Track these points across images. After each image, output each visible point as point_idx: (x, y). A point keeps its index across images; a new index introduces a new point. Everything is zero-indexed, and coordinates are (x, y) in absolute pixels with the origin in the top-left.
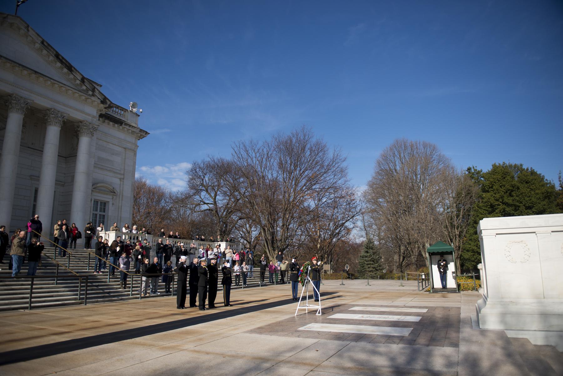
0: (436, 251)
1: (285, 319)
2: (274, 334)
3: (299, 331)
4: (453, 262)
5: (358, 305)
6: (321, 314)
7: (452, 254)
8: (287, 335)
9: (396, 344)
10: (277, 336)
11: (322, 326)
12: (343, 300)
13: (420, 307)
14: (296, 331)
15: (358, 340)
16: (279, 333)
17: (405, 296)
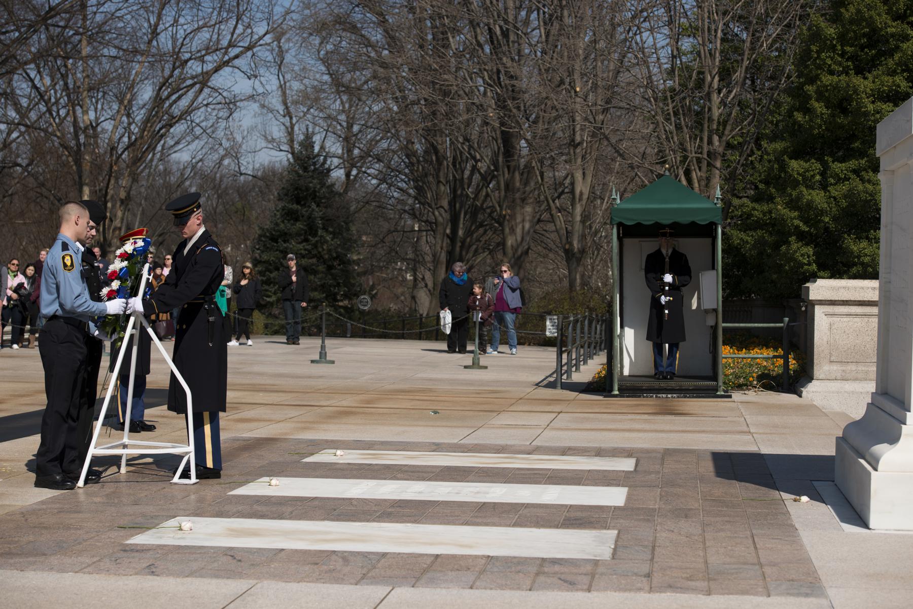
0: (648, 221)
1: (42, 502)
2: (35, 563)
3: (137, 551)
4: (713, 268)
5: (332, 441)
6: (193, 479)
7: (714, 238)
8: (95, 568)
9: (582, 590)
10: (51, 569)
11: (232, 530)
12: (261, 424)
13: (599, 453)
14: (125, 551)
15: (418, 579)
16: (54, 560)
17: (512, 408)
